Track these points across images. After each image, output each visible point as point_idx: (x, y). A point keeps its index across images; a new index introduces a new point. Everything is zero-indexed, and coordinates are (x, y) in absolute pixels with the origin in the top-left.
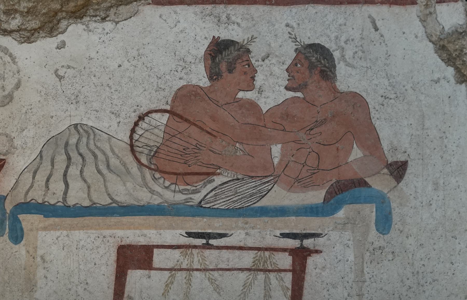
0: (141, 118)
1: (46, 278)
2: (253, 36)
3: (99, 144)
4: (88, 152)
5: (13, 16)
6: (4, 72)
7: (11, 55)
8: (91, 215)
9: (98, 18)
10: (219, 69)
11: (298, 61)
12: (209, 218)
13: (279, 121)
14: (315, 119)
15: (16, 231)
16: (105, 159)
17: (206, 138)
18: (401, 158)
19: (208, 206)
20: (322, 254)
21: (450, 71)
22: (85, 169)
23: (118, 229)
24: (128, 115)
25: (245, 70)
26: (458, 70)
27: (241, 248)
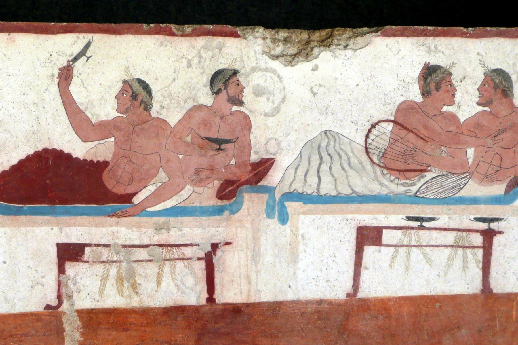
0: (373, 126)
1: (306, 252)
2: (453, 62)
3: (343, 147)
4: (334, 152)
5: (277, 44)
6: (274, 89)
7: (278, 76)
9: (342, 46)
10: (429, 88)
11: (485, 82)
12: (421, 205)
13: (472, 129)
14: (498, 129)
15: (283, 214)
16: (347, 159)
17: (421, 143)
19: (421, 196)
20: (504, 234)
22: (333, 167)
23: (357, 213)
24: (364, 124)
25: (448, 89)
27: (446, 229)
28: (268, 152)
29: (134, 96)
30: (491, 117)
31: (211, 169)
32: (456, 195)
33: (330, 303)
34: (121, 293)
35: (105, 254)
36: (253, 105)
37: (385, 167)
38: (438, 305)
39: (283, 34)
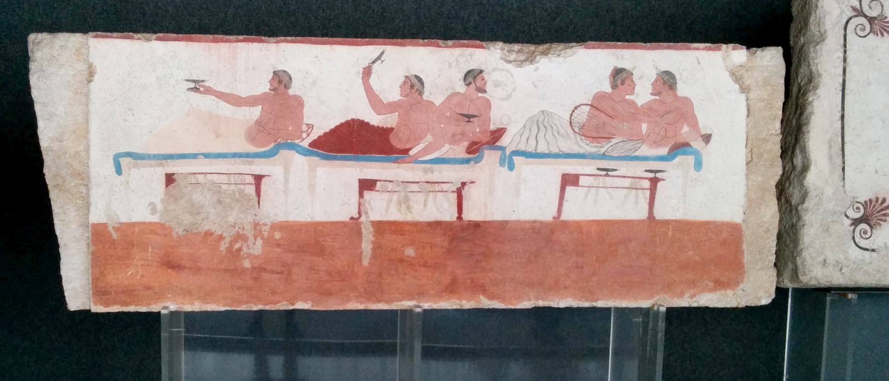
0: (576, 108)
17: (608, 119)
18: (708, 132)
21: (738, 86)
26: (741, 87)
27: (624, 177)
28: (502, 123)
29: (412, 86)
31: (463, 134)
33: (541, 223)
34: (399, 211)
35: (390, 186)
36: (493, 93)
37: (583, 135)
38: (616, 226)
39: (516, 47)
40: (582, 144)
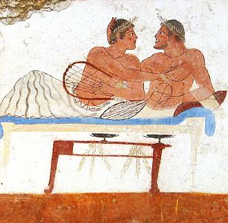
0: (70, 67)
8: (41, 123)
17: (108, 78)
27: (124, 143)
30: (165, 57)
32: (135, 117)
33: (32, 196)
40: (77, 108)
